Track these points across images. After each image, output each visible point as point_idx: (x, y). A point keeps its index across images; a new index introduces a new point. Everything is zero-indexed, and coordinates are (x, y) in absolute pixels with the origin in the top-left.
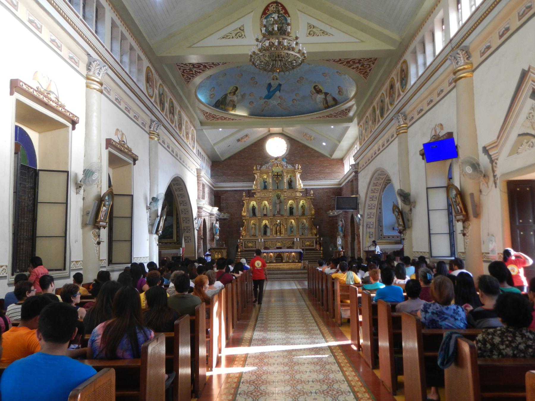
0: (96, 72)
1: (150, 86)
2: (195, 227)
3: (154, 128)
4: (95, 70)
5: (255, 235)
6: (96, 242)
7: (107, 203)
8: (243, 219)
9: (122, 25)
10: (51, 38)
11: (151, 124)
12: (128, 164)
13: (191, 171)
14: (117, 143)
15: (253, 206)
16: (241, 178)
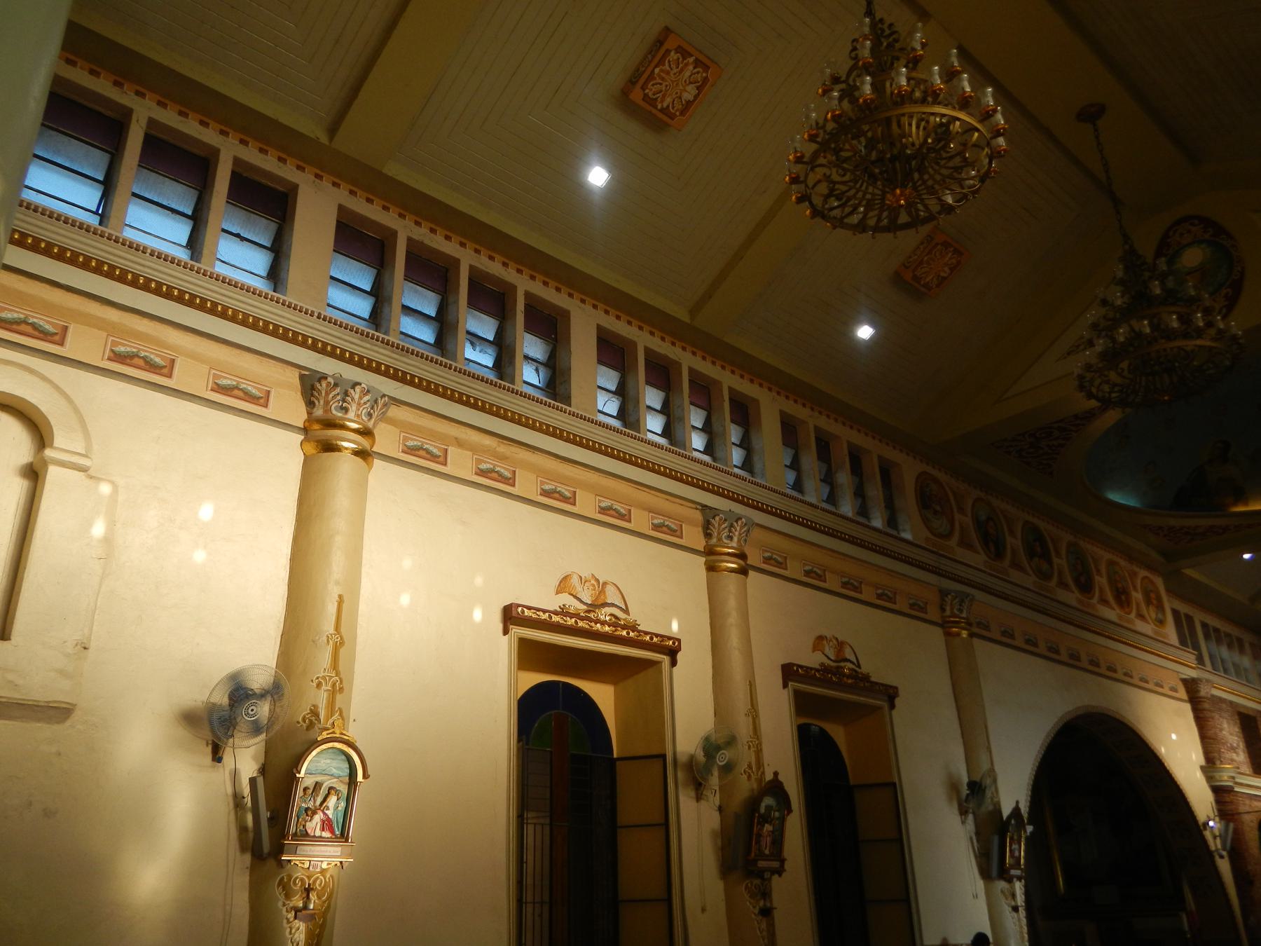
0: (723, 537)
1: (936, 512)
2: (1213, 848)
3: (952, 609)
4: (719, 534)
6: (756, 911)
7: (777, 814)
9: (816, 414)
10: (599, 506)
11: (944, 600)
12: (875, 709)
13: (1160, 690)
14: (811, 669)
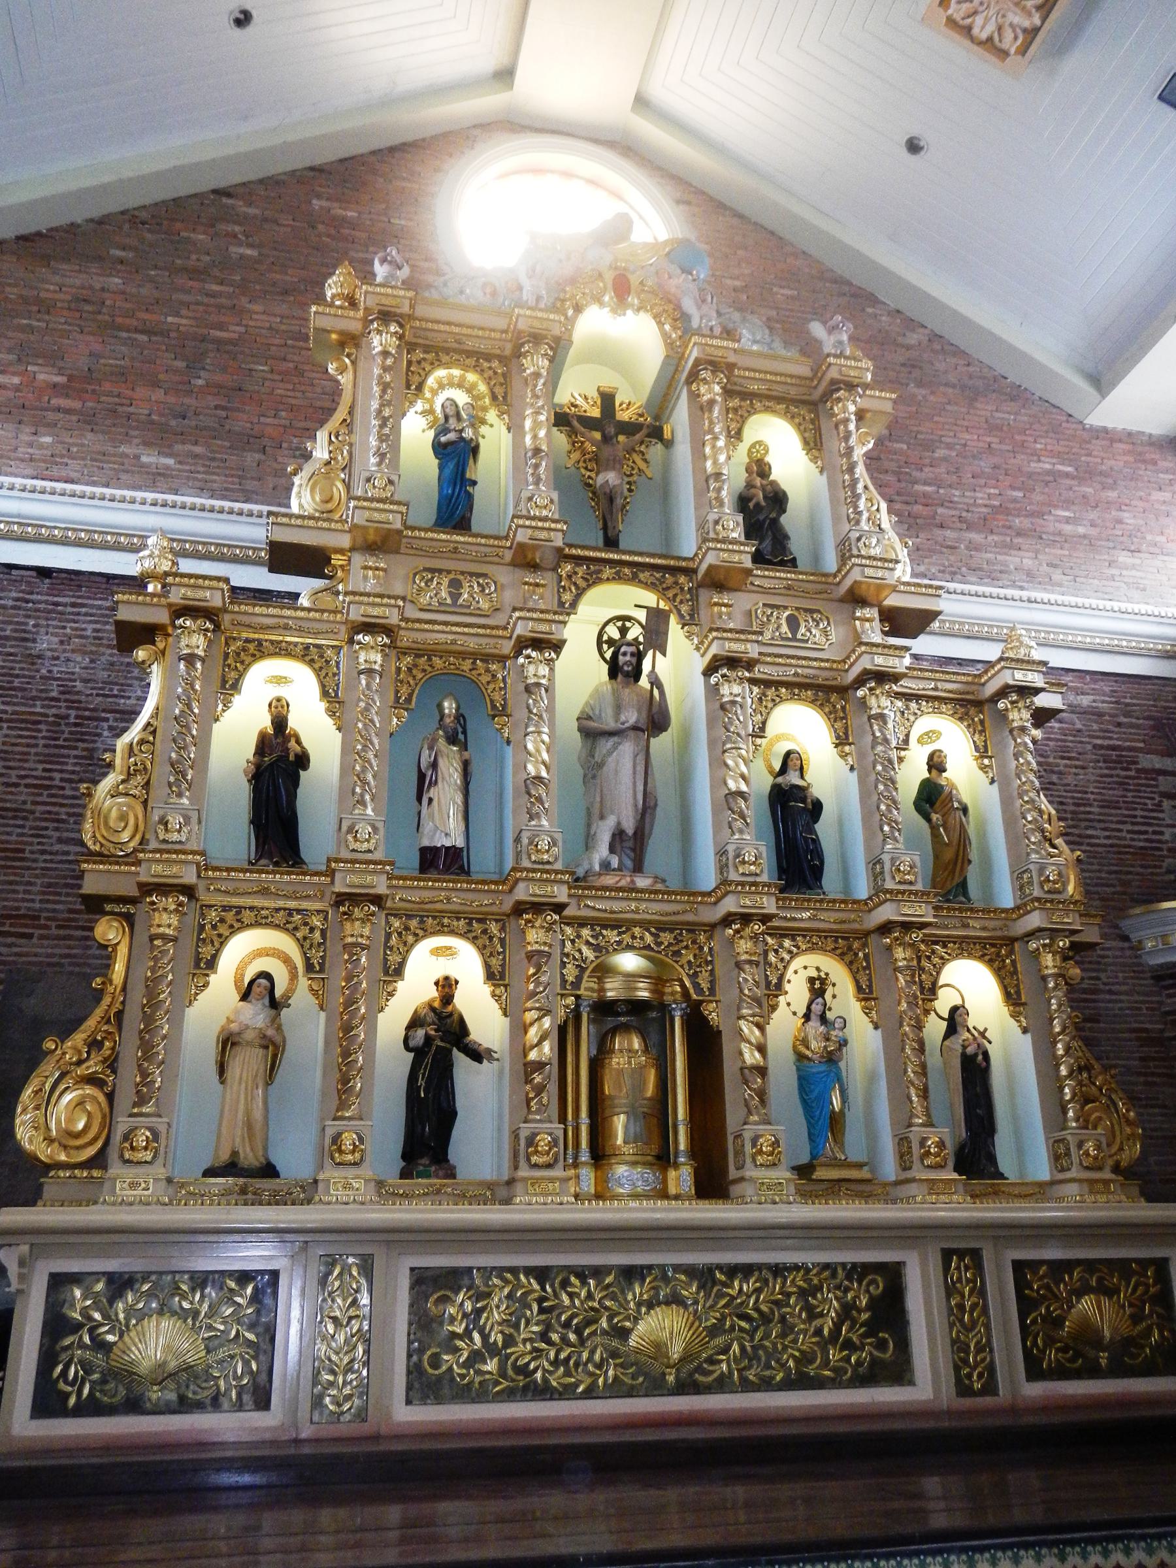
5: (269, 1171)
8: (96, 905)
15: (280, 723)
16: (149, 458)
